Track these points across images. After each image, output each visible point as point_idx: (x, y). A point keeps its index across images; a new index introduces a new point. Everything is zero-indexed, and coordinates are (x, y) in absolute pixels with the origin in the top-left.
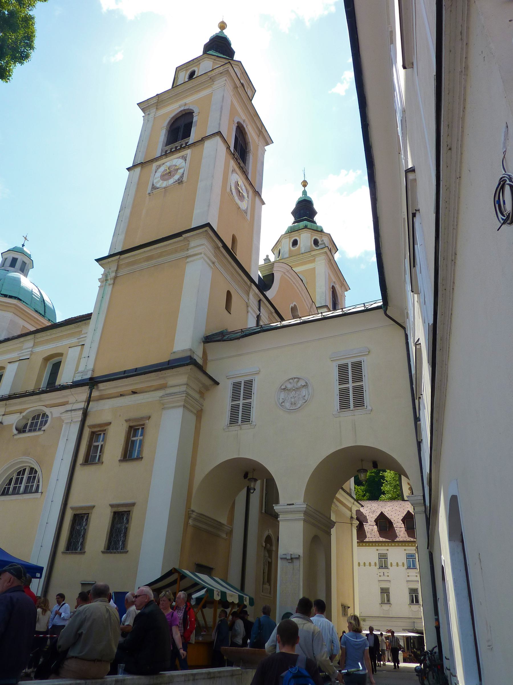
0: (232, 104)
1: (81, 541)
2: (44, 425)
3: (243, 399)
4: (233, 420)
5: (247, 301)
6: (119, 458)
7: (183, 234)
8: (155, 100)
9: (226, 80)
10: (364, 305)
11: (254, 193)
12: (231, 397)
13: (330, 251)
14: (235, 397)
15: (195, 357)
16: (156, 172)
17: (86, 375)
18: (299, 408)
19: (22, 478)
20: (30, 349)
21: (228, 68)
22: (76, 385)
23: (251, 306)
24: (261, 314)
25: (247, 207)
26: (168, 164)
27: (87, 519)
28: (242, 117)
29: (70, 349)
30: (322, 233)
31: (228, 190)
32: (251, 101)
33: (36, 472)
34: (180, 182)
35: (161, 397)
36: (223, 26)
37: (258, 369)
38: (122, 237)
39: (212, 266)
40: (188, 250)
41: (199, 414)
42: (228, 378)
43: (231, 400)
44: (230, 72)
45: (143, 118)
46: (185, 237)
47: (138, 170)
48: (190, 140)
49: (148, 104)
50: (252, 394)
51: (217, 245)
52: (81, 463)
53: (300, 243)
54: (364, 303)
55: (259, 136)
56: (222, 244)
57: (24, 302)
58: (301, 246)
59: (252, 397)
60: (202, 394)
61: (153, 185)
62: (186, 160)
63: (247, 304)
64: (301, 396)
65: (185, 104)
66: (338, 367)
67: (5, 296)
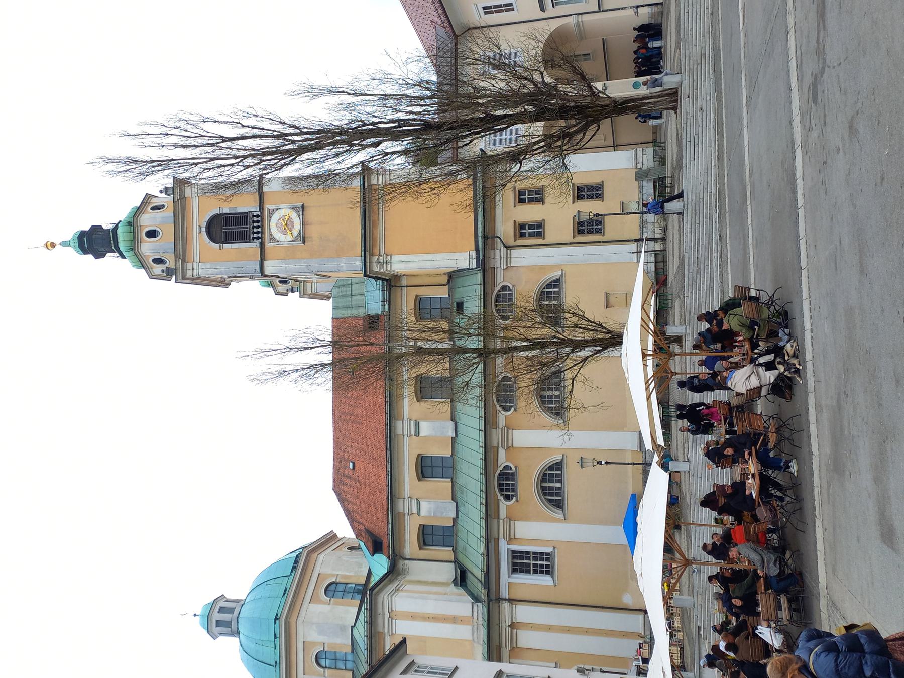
52: (542, 240)
61: (293, 241)
65: (200, 227)
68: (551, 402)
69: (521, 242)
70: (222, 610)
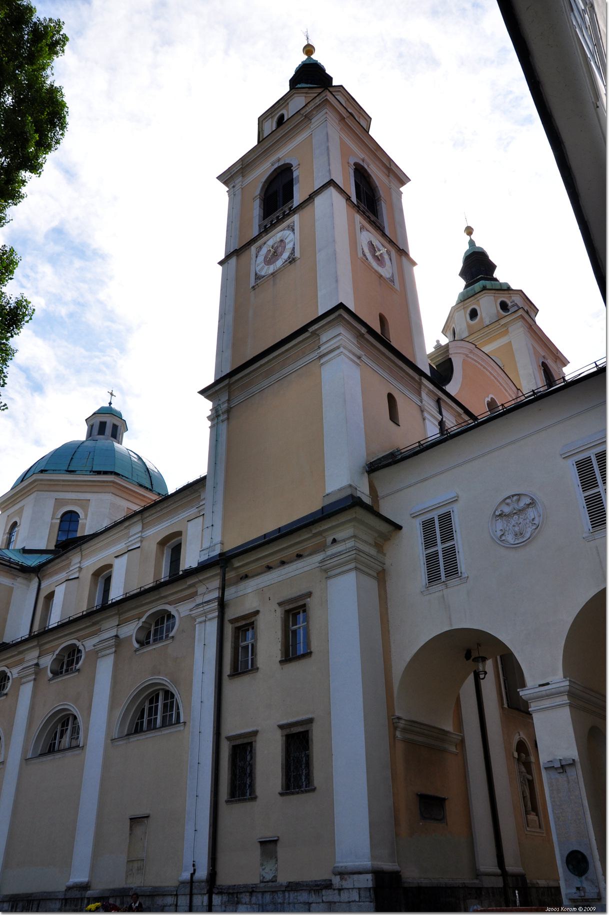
0: (342, 143)
1: (248, 782)
2: (172, 631)
3: (442, 543)
4: (433, 577)
5: (419, 403)
6: (279, 658)
7: (309, 328)
8: (238, 165)
9: (326, 113)
10: (596, 364)
11: (399, 253)
12: (423, 543)
13: (527, 312)
14: (429, 541)
15: (359, 494)
16: (257, 257)
17: (214, 550)
18: (529, 538)
19: (157, 707)
20: (139, 535)
21: (326, 96)
22: (203, 567)
23: (428, 409)
24: (444, 419)
25: (393, 273)
26: (271, 243)
27: (251, 751)
28: (359, 155)
29: (189, 523)
30: (510, 292)
31: (360, 255)
32: (368, 132)
33: (173, 696)
34: (292, 260)
35: (321, 562)
36: (309, 50)
37: (456, 495)
38: (228, 353)
39: (359, 363)
40: (319, 348)
41: (381, 577)
42: (413, 517)
43: (424, 548)
44: (330, 100)
45: (227, 194)
46: (312, 330)
47: (233, 260)
48: (294, 203)
49: (230, 173)
50: (454, 532)
51: (359, 331)
52: (229, 673)
53: (481, 314)
54: (595, 362)
55: (389, 176)
56: (367, 329)
57: (123, 476)
58: (483, 317)
59: (455, 537)
60: (379, 547)
61: (256, 274)
62: (293, 230)
63: (421, 409)
64: (528, 521)
65: (279, 160)
66: (577, 465)
67: (99, 473)
69: (229, 630)
70: (115, 427)
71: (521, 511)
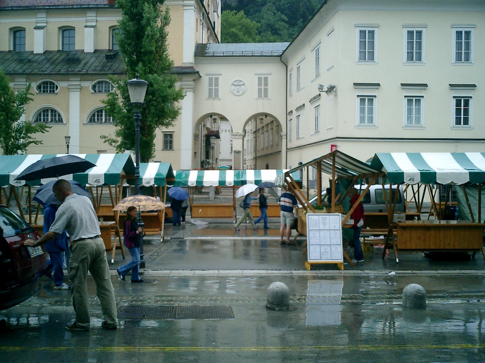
4: (210, 96)
14: (210, 84)
68: (44, 116)
71: (239, 85)
